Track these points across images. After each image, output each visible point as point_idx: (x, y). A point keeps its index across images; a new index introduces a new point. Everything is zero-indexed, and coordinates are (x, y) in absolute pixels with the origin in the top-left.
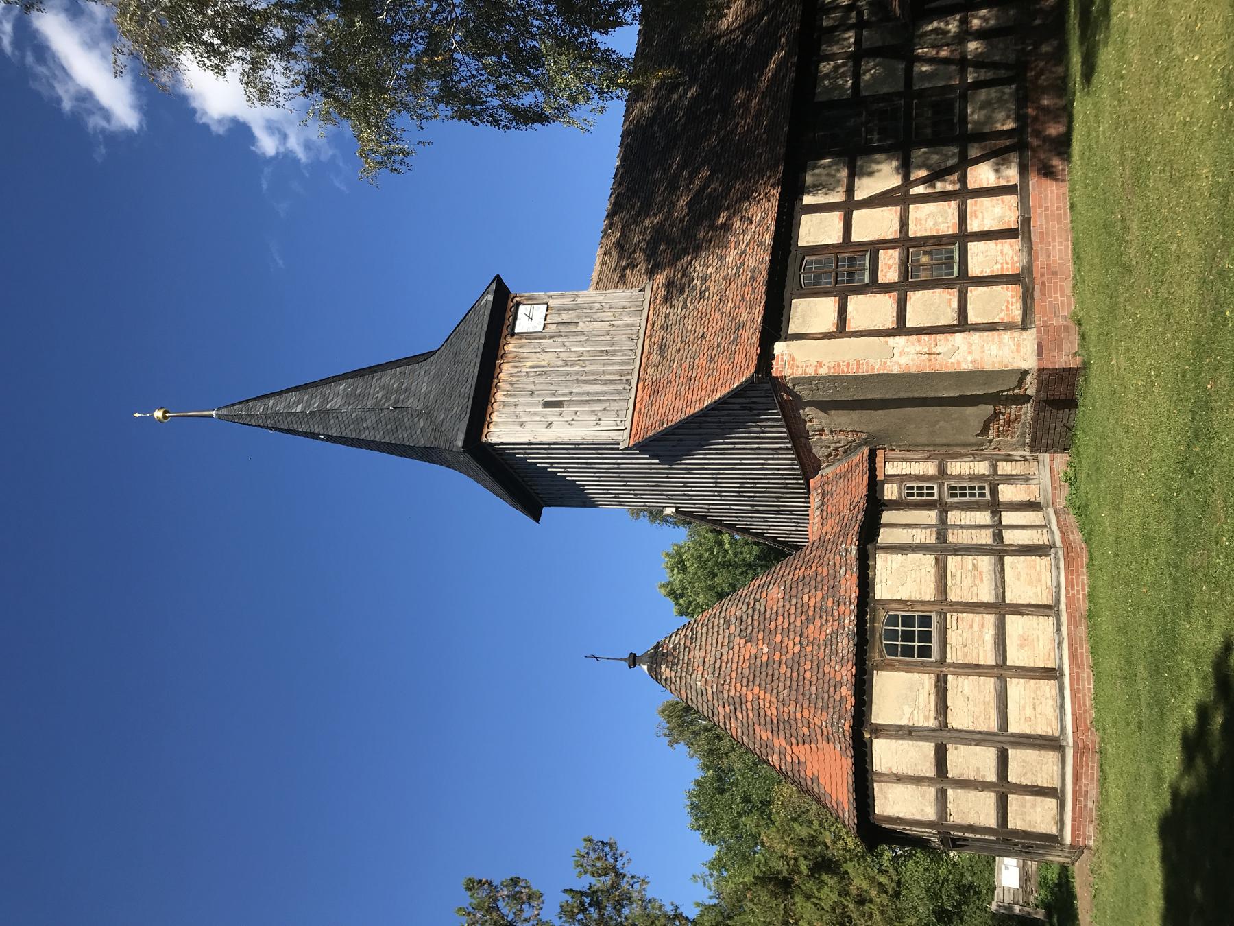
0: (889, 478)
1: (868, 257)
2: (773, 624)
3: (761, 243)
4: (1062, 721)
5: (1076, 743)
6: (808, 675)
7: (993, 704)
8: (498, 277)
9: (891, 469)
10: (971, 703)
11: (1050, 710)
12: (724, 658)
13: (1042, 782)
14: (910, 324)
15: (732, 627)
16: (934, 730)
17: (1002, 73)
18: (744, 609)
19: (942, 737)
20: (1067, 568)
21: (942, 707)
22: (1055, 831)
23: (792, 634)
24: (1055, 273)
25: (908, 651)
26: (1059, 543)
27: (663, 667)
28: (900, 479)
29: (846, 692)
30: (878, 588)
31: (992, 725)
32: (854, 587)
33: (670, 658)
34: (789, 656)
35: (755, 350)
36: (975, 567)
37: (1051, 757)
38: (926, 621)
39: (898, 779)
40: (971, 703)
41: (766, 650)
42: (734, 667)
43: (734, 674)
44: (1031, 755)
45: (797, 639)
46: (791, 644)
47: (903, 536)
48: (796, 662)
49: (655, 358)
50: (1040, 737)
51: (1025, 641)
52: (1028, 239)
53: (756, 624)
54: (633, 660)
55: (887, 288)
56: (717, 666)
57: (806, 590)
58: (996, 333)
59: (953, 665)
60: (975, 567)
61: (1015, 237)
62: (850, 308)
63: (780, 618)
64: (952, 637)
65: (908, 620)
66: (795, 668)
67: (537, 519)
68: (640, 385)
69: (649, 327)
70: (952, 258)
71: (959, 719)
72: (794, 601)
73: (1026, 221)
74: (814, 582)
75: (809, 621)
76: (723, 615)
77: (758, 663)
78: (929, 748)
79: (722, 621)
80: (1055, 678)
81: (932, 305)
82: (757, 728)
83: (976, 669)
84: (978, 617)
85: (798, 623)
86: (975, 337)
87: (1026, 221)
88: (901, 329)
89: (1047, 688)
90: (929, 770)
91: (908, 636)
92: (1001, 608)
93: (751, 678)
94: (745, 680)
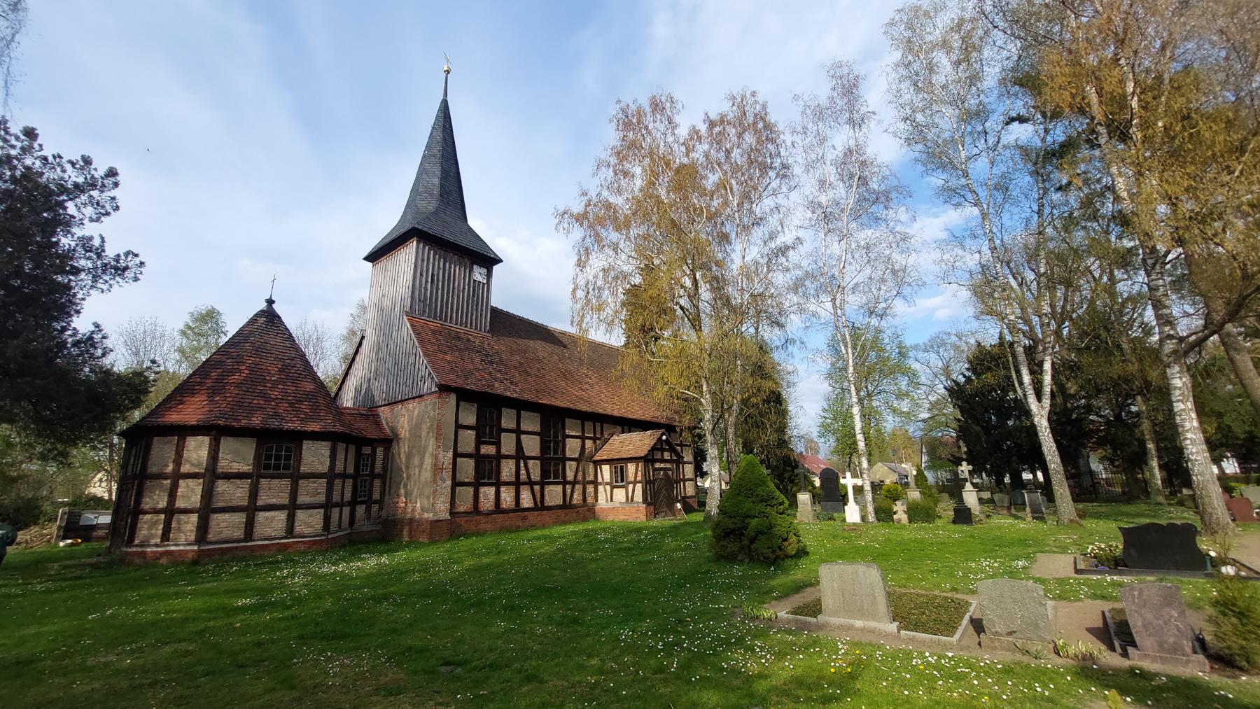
11: (226, 534)
25: (268, 458)
35: (453, 384)
38: (287, 467)
47: (340, 456)
55: (478, 448)
59: (258, 483)
64: (276, 482)
65: (288, 458)
67: (366, 259)
81: (467, 468)
86: (449, 489)
88: (456, 455)
89: (239, 533)
91: (278, 458)
92: (292, 508)
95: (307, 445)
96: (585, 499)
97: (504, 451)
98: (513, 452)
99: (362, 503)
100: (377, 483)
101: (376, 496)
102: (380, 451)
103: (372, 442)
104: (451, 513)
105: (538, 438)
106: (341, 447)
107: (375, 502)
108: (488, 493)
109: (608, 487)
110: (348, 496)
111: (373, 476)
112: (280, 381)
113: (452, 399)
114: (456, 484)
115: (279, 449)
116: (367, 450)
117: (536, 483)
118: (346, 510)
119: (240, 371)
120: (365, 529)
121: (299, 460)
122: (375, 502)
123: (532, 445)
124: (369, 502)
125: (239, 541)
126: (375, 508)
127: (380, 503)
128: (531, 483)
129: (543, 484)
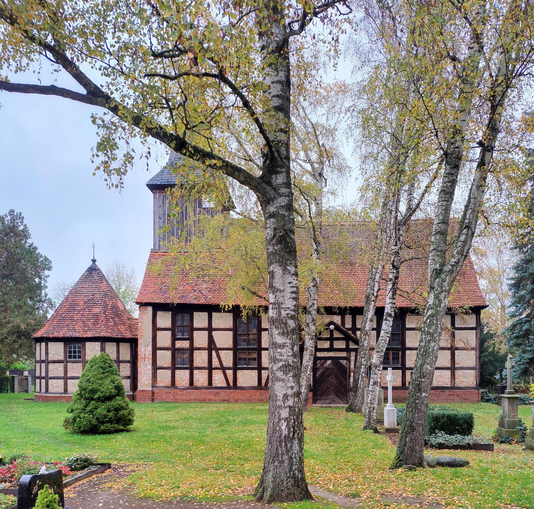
5: (47, 396)
6: (66, 323)
7: (56, 376)
10: (56, 370)
11: (55, 390)
17: (263, 382)
21: (54, 362)
24: (174, 396)
25: (70, 352)
29: (56, 335)
30: (89, 343)
38: (79, 357)
40: (56, 370)
48: (72, 319)
50: (48, 388)
52: (187, 388)
54: (94, 261)
55: (173, 344)
59: (67, 365)
62: (166, 332)
71: (51, 366)
73: (196, 388)
75: (84, 322)
76: (98, 293)
81: (165, 358)
83: (66, 371)
86: (150, 372)
87: (196, 388)
89: (62, 390)
91: (75, 352)
95: (88, 344)
97: (196, 344)
98: (205, 344)
104: (153, 387)
105: (231, 333)
108: (182, 376)
112: (83, 309)
113: (150, 309)
114: (155, 368)
115: (75, 348)
117: (229, 369)
121: (85, 354)
123: (225, 339)
125: (62, 394)
128: (223, 369)
129: (235, 369)
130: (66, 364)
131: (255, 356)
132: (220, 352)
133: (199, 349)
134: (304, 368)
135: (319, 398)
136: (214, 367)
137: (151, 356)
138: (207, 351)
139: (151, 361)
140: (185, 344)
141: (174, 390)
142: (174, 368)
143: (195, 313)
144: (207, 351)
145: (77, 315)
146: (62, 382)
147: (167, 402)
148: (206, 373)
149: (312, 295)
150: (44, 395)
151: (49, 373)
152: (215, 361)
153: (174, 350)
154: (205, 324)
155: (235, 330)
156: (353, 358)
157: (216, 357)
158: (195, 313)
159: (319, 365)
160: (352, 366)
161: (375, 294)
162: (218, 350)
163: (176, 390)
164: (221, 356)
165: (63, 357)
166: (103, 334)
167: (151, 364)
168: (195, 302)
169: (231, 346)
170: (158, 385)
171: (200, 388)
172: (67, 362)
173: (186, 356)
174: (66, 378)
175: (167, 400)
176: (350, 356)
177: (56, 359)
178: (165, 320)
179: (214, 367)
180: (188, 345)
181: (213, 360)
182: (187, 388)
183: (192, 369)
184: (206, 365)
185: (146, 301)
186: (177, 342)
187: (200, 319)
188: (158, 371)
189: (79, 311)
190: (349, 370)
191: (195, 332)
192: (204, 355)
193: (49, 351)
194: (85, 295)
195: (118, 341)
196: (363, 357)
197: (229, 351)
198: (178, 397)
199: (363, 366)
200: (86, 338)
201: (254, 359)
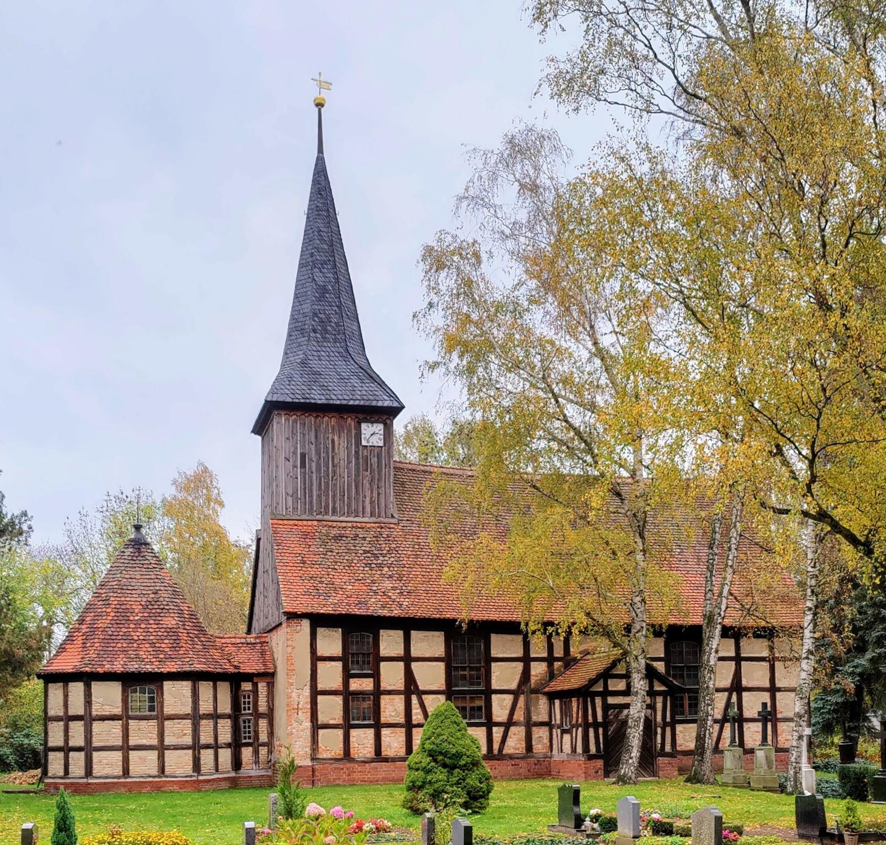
0: (255, 685)
1: (369, 672)
2: (152, 622)
3: (383, 607)
4: (100, 777)
5: (90, 784)
6: (120, 645)
7: (107, 744)
8: (404, 407)
9: (260, 685)
12: (134, 592)
13: (71, 768)
14: (320, 698)
15: (153, 596)
16: (90, 715)
17: (496, 747)
18: (164, 603)
19: (88, 719)
20: (187, 781)
21: (103, 718)
22: (50, 775)
23: (144, 634)
26: (201, 778)
27: (131, 550)
28: (255, 691)
29: (108, 668)
30: (171, 682)
31: (96, 743)
32: (168, 670)
33: (137, 554)
34: (132, 634)
35: (301, 609)
36: (185, 734)
37: (82, 772)
39: (66, 696)
40: (107, 733)
41: (136, 618)
42: (128, 599)
43: (123, 599)
44: (82, 763)
45: (141, 638)
46: (138, 634)
48: (128, 638)
49: (334, 532)
50: (91, 767)
51: (143, 760)
52: (372, 761)
53: (154, 611)
55: (346, 684)
56: (130, 588)
57: (171, 641)
58: (309, 744)
59: (127, 724)
60: (185, 734)
61: (376, 755)
62: (333, 663)
63: (156, 626)
64: (144, 723)
66: (124, 637)
68: (315, 523)
69: (359, 525)
70: (364, 719)
71: (97, 727)
72: (165, 634)
73: (386, 760)
74: (175, 647)
75: (153, 644)
76: (162, 588)
77: (128, 614)
78: (81, 712)
79: (158, 588)
80: (124, 775)
81: (331, 709)
82: (92, 614)
84: (155, 736)
85: (151, 638)
86: (308, 733)
87: (386, 760)
88: (315, 693)
89: (119, 771)
90: (71, 712)
92: (161, 748)
93: (121, 610)
94: (118, 606)
95: (167, 685)
96: (529, 747)
97: (385, 685)
98: (400, 685)
99: (248, 745)
100: (263, 724)
101: (263, 737)
102: (262, 687)
103: (249, 677)
104: (312, 759)
105: (442, 665)
106: (205, 689)
107: (263, 745)
108: (362, 741)
109: (559, 731)
110: (226, 736)
111: (258, 715)
112: (145, 620)
113: (306, 624)
114: (316, 726)
116: (247, 686)
118: (225, 755)
119: (108, 614)
120: (253, 773)
121: (162, 703)
122: (263, 745)
123: (431, 676)
124: (256, 745)
125: (119, 777)
126: (263, 751)
127: (269, 745)
130: (127, 721)
131: (480, 703)
132: (424, 697)
133: (389, 692)
134: (635, 721)
135: (612, 768)
136: (414, 722)
137: (309, 706)
138: (403, 696)
139: (309, 714)
140: (366, 685)
141: (348, 765)
142: (347, 727)
143: (381, 631)
144: (403, 696)
145: (135, 630)
146: (118, 756)
147: (339, 785)
148: (401, 733)
149: (640, 615)
150: (85, 780)
151: (760, 729)
152: (417, 714)
153: (347, 695)
154: (400, 651)
155: (447, 660)
156: (659, 706)
157: (418, 706)
158: (382, 632)
159: (612, 717)
160: (659, 718)
161: (722, 613)
162: (420, 693)
163: (352, 765)
164: (426, 704)
165: (120, 709)
166: (199, 667)
167: (309, 719)
168: (385, 613)
169: (444, 688)
170: (321, 757)
171: (394, 760)
172: (129, 718)
173: (368, 704)
174: (126, 748)
175: (337, 782)
176: (655, 703)
177: (108, 713)
178: (331, 642)
179: (414, 722)
180: (372, 685)
181: (414, 711)
182: (372, 761)
183: (378, 727)
184: (402, 720)
185: (304, 611)
186: (352, 681)
187: (390, 643)
188: (321, 732)
189: (137, 624)
190: (655, 724)
191: (382, 664)
192: (399, 702)
193: (93, 698)
194: (139, 592)
195: (214, 678)
196: (708, 705)
197: (439, 696)
198: (355, 776)
199: (710, 718)
200: (169, 673)
201: (480, 708)
